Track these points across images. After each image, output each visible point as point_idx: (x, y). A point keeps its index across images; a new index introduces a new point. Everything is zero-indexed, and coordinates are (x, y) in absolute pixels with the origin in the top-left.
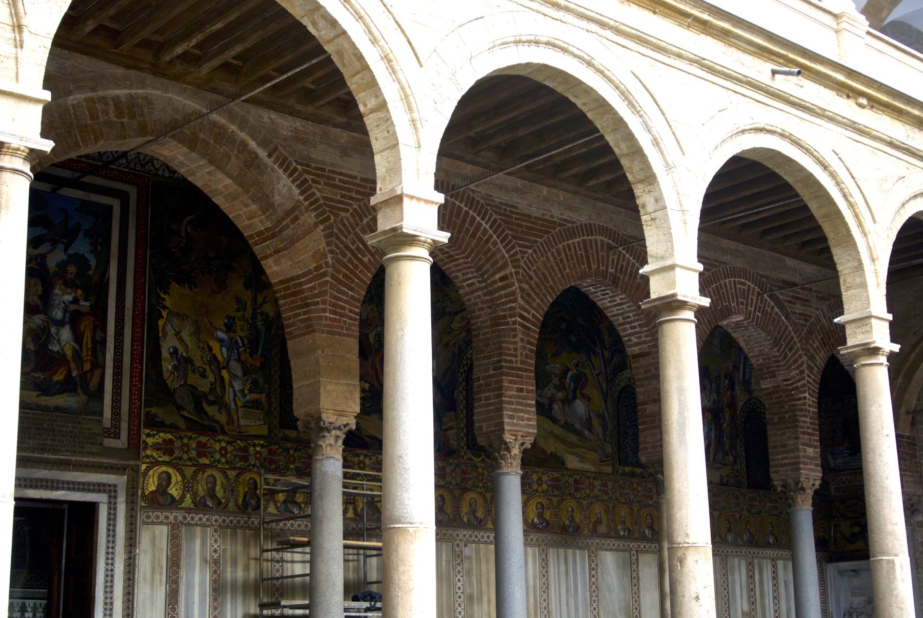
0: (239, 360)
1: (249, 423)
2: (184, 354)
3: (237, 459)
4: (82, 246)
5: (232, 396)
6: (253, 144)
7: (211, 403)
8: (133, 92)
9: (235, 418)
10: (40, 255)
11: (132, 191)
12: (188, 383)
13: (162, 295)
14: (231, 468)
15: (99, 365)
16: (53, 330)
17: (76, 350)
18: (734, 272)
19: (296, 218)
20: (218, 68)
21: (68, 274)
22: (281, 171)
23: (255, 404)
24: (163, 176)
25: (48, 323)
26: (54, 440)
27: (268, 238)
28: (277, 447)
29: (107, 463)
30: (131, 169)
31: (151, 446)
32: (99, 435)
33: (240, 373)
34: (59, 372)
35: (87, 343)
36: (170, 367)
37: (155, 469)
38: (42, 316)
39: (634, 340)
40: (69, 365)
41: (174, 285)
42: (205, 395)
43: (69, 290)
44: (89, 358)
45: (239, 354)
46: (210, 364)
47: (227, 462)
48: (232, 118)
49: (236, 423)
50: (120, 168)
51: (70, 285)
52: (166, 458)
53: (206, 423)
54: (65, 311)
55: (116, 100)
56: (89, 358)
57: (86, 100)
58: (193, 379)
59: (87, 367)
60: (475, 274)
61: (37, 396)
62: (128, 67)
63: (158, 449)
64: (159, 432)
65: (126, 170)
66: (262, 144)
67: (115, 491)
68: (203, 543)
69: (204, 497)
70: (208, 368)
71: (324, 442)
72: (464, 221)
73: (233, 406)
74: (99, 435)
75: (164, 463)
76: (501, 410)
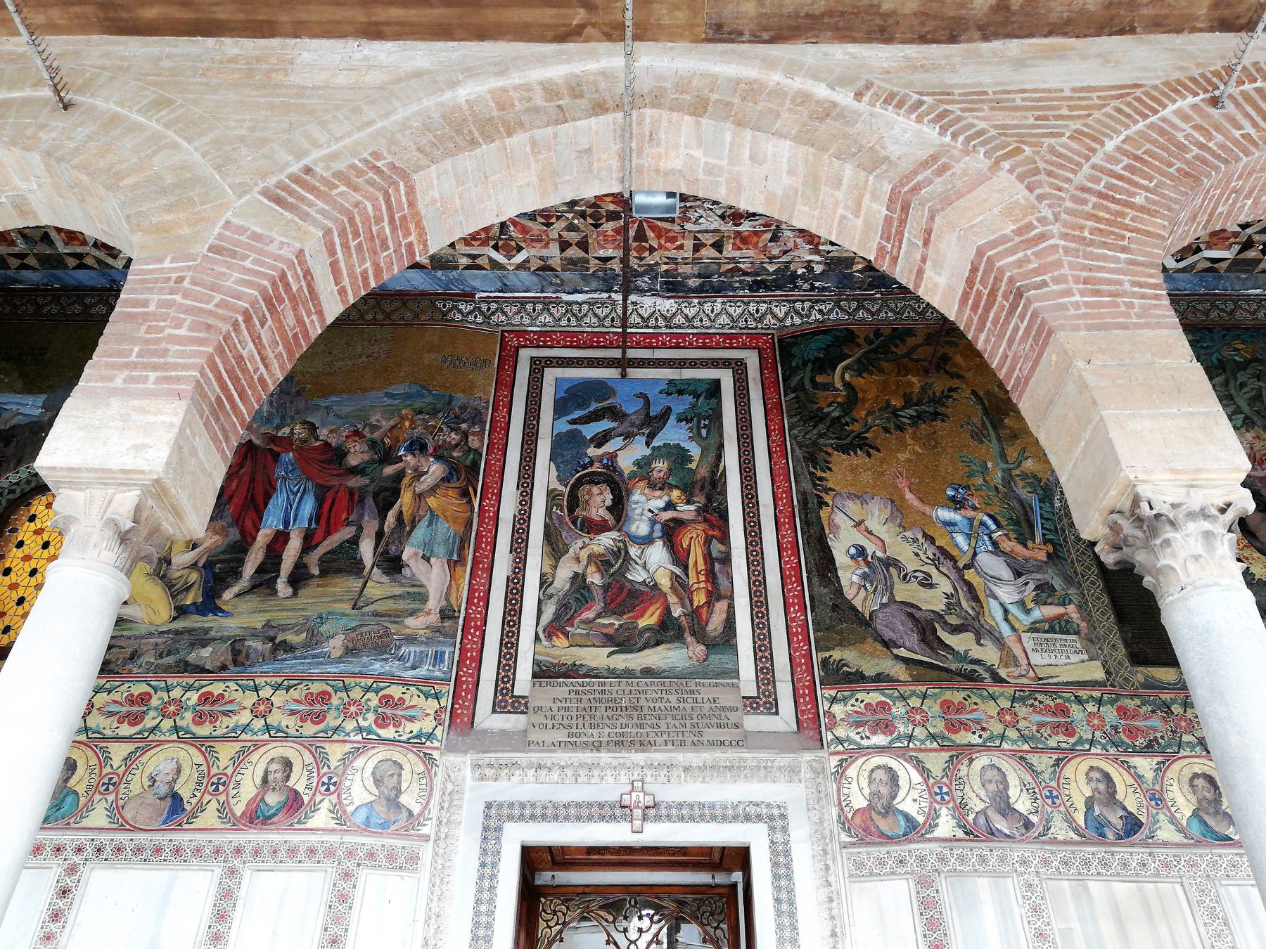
0: (996, 548)
1: (1053, 661)
2: (879, 554)
3: (1046, 731)
4: (674, 434)
5: (999, 615)
7: (956, 630)
9: (1017, 651)
11: (752, 359)
12: (898, 599)
13: (819, 474)
14: (1035, 750)
15: (719, 592)
16: (634, 551)
17: (677, 576)
23: (1059, 626)
24: (793, 325)
26: (641, 726)
27: (903, 222)
28: (1137, 701)
30: (741, 329)
31: (842, 720)
32: (732, 709)
33: (1006, 573)
34: (649, 613)
35: (696, 563)
36: (855, 579)
37: (859, 762)
38: (614, 534)
40: (666, 599)
41: (838, 456)
43: (658, 493)
44: (702, 585)
45: (995, 544)
46: (936, 563)
47: (1024, 738)
49: (1023, 661)
50: (725, 331)
52: (880, 739)
53: (954, 667)
56: (702, 585)
58: (904, 592)
59: (700, 599)
63: (858, 724)
64: (854, 691)
65: (733, 331)
69: (984, 812)
70: (933, 571)
71: (1174, 556)
73: (1005, 629)
74: (732, 709)
75: (880, 750)
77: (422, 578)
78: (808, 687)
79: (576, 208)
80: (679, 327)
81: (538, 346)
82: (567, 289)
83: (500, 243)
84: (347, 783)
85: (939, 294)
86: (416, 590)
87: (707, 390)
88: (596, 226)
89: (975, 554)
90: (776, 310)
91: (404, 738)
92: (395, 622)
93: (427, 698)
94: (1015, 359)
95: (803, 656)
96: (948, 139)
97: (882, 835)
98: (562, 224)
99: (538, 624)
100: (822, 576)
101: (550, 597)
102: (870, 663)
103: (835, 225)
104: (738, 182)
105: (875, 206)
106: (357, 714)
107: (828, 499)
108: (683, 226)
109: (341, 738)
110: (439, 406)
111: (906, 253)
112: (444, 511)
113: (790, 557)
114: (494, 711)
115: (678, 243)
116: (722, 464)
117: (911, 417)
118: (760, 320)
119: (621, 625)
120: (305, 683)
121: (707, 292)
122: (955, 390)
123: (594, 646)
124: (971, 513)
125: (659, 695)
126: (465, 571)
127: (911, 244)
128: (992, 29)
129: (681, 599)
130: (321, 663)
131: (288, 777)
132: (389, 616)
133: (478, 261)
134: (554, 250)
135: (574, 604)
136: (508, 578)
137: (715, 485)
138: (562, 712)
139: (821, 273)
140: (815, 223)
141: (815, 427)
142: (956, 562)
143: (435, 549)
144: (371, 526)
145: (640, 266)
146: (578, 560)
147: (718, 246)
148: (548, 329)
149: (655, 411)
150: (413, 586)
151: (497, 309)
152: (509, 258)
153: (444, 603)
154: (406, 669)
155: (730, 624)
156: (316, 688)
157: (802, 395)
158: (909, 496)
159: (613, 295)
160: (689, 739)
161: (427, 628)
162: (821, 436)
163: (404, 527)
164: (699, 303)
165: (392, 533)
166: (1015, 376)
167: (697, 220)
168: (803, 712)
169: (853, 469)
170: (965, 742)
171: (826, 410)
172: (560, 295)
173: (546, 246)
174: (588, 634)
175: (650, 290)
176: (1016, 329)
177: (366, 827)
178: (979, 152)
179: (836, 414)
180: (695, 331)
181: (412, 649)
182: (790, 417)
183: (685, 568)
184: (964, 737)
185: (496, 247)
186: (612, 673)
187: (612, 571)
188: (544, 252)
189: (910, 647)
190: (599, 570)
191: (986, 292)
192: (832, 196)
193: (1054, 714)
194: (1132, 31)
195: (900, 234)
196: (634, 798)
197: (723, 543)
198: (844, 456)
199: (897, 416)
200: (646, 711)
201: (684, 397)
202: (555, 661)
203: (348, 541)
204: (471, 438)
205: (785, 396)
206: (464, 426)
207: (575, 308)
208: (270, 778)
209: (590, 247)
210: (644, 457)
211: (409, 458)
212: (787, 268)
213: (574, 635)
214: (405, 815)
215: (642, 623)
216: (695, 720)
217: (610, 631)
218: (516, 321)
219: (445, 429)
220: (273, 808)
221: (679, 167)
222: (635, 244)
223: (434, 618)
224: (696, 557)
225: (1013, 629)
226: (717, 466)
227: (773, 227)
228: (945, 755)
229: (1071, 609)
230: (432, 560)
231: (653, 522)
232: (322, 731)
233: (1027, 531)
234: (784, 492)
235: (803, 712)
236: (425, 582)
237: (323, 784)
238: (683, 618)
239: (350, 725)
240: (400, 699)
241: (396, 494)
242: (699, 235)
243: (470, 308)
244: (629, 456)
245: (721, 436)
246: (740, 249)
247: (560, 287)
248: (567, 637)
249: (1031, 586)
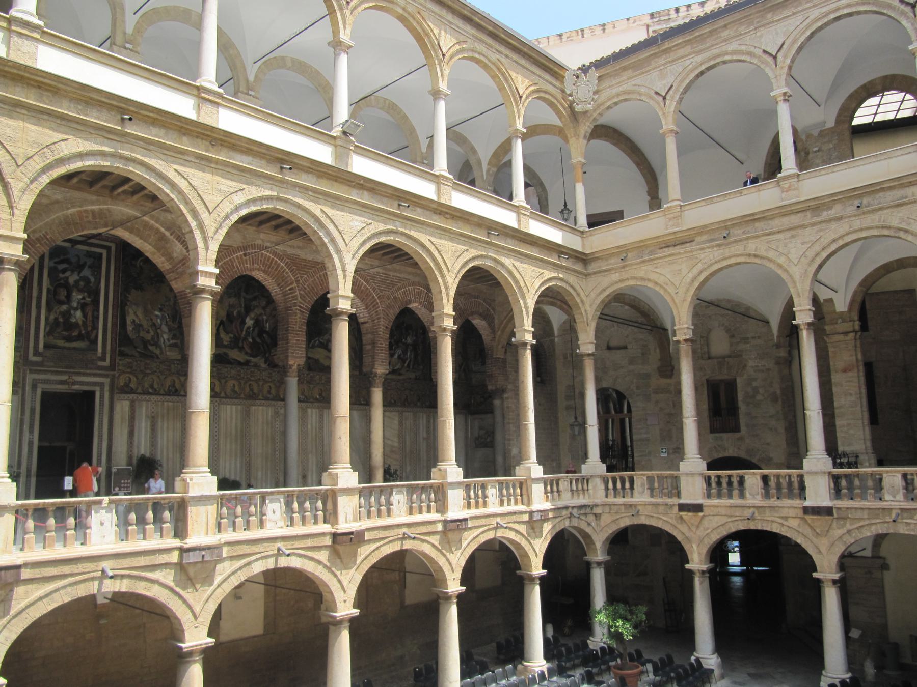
0: (167, 324)
4: (86, 272)
6: (162, 230)
7: (152, 345)
8: (101, 207)
11: (113, 246)
15: (95, 328)
16: (72, 312)
18: (413, 284)
19: (185, 263)
20: (142, 196)
22: (177, 242)
38: (67, 306)
39: (361, 315)
41: (133, 290)
42: (149, 341)
45: (167, 322)
48: (152, 217)
51: (80, 291)
52: (129, 370)
55: (93, 212)
57: (77, 212)
58: (142, 334)
59: (89, 329)
62: (98, 196)
66: (168, 229)
68: (147, 408)
72: (271, 262)
73: (163, 346)
76: (288, 349)
149: (82, 262)
155: (97, 336)
183: (86, 319)
184: (148, 371)
186: (64, 348)
215: (74, 334)
224: (90, 315)
231: (78, 303)
244: (73, 279)
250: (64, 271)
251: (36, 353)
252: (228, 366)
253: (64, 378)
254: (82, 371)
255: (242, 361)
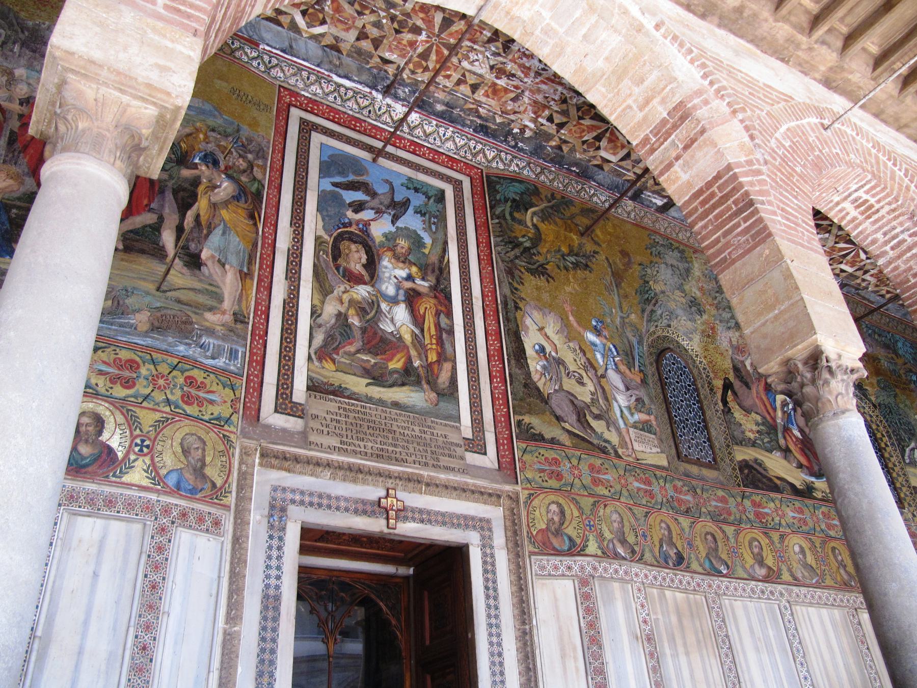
0: (617, 370)
2: (553, 354)
3: (641, 494)
4: (411, 221)
7: (597, 417)
9: (628, 440)
10: (361, 220)
13: (516, 285)
14: (635, 504)
15: (446, 356)
16: (384, 306)
17: (416, 335)
21: (399, 248)
24: (497, 168)
25: (377, 297)
26: (395, 446)
27: (675, 127)
29: (474, 485)
32: (458, 445)
33: (621, 387)
34: (396, 359)
36: (539, 368)
40: (408, 351)
41: (527, 276)
43: (401, 265)
44: (434, 347)
49: (630, 447)
51: (402, 259)
52: (553, 483)
53: (595, 442)
54: (398, 288)
58: (569, 385)
59: (433, 357)
60: (906, 225)
61: (368, 385)
67: (490, 530)
68: (627, 608)
69: (611, 541)
70: (584, 375)
71: (830, 392)
77: (217, 278)
78: (506, 439)
79: (392, 11)
80: (418, 137)
81: (306, 110)
82: (340, 72)
83: (311, 11)
84: (159, 448)
85: (676, 185)
86: (213, 289)
87: (436, 195)
88: (397, 32)
89: (606, 369)
90: (487, 153)
91: (206, 418)
92: (196, 313)
93: (224, 387)
94: (727, 245)
95: (503, 416)
96: (706, 83)
97: (554, 549)
98: (372, 18)
99: (310, 346)
100: (518, 361)
101: (320, 326)
102: (551, 431)
103: (619, 110)
104: (562, 48)
105: (660, 109)
106: (165, 388)
107: (521, 305)
108: (460, 62)
109: (151, 406)
110: (229, 130)
111: (665, 149)
112: (235, 226)
113: (494, 341)
114: (276, 411)
115: (449, 73)
116: (446, 257)
117: (572, 263)
118: (475, 155)
119: (376, 364)
120: (114, 348)
121: (444, 119)
122: (597, 253)
123: (355, 375)
124: (605, 341)
125: (406, 425)
126: (253, 285)
127: (673, 143)
128: (726, 22)
129: (419, 354)
130: (129, 333)
131: (100, 433)
132: (190, 306)
133: (282, 18)
134: (351, 36)
135: (339, 337)
136: (284, 300)
137: (442, 272)
138: (334, 423)
139: (528, 138)
140: (605, 102)
141: (512, 249)
142: (596, 371)
143: (229, 257)
144: (171, 219)
145: (409, 78)
146: (342, 303)
147: (474, 88)
148: (317, 99)
149: (398, 198)
150: (211, 285)
151: (277, 65)
152: (309, 25)
153: (237, 307)
154: (207, 357)
156: (124, 355)
157: (503, 222)
158: (571, 318)
159: (374, 92)
160: (431, 462)
161: (223, 325)
162: (517, 257)
163: (203, 229)
164: (437, 125)
165: (191, 231)
166: (723, 256)
167: (473, 61)
168: (503, 457)
169: (538, 288)
170: (602, 493)
171: (521, 239)
172: (331, 75)
173: (347, 30)
174: (350, 364)
175: (404, 100)
176: (738, 225)
177: (177, 490)
178: (724, 100)
179: (528, 244)
180: (429, 146)
181: (211, 341)
182: (495, 236)
183: (422, 331)
185: (304, 13)
187: (368, 317)
188: (342, 35)
189: (571, 423)
190: (358, 315)
191: (720, 195)
192: (630, 88)
193: (645, 483)
194: (787, 62)
195: (668, 134)
196: (389, 503)
197: (448, 318)
198: (532, 277)
199: (564, 259)
200: (397, 434)
201: (419, 194)
202: (325, 380)
203: (150, 226)
204: (255, 169)
205: (492, 219)
206: (250, 156)
207: (342, 90)
208: (83, 429)
209: (382, 46)
210: (390, 232)
211: (204, 168)
212: (509, 124)
213: (339, 362)
214: (208, 485)
216: (433, 449)
217: (368, 366)
218: (292, 81)
219: (235, 153)
220: (86, 458)
221: (526, 19)
222: (417, 59)
223: (228, 318)
224: (429, 322)
225: (625, 424)
226: (443, 257)
227: (519, 91)
228: (591, 500)
229: (652, 417)
230: (227, 267)
232: (132, 396)
233: (631, 360)
234: (489, 291)
235: (503, 457)
236: (221, 285)
237: (137, 445)
238: (420, 369)
239: (159, 396)
240: (202, 383)
241: (194, 197)
242: (467, 74)
243: (254, 54)
245: (446, 235)
246: (488, 96)
247: (336, 69)
248: (334, 363)
249: (634, 398)
250: (358, 207)
251: (284, 404)
252: (773, 495)
253: (372, 492)
254: (425, 473)
255: (798, 484)
